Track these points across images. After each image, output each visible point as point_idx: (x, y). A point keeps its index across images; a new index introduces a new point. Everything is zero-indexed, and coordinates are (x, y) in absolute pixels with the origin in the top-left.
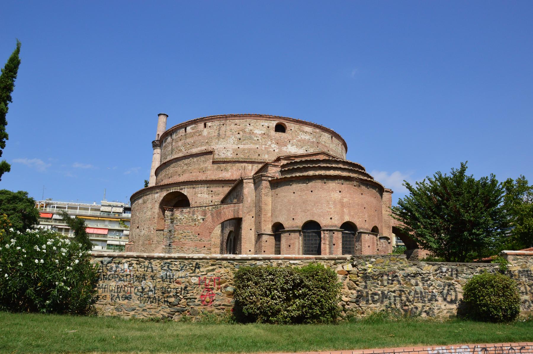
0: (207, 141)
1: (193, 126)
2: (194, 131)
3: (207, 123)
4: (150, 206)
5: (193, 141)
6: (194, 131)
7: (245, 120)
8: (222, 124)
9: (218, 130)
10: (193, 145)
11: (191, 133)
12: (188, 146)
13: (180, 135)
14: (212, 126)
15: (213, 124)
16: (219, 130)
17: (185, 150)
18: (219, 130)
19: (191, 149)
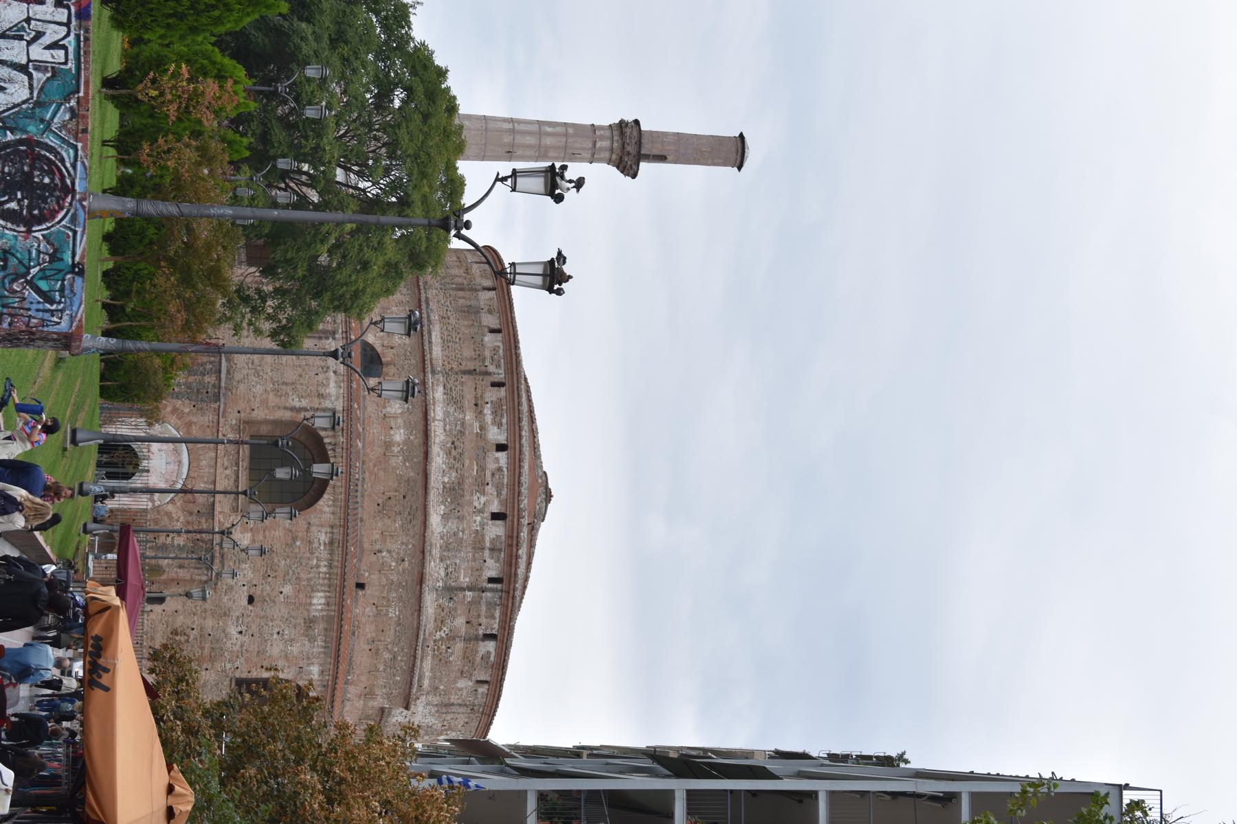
0: (442, 687)
1: (492, 659)
2: (478, 659)
3: (486, 686)
4: (295, 649)
5: (451, 659)
6: (478, 659)
7: (473, 730)
8: (475, 708)
9: (460, 701)
10: (442, 661)
11: (477, 652)
12: (444, 647)
13: (483, 620)
14: (476, 694)
15: (479, 696)
16: (460, 705)
17: (435, 641)
18: (460, 705)
19: (434, 656)
